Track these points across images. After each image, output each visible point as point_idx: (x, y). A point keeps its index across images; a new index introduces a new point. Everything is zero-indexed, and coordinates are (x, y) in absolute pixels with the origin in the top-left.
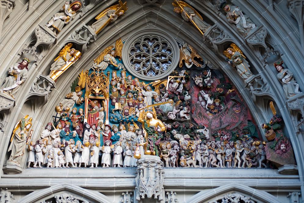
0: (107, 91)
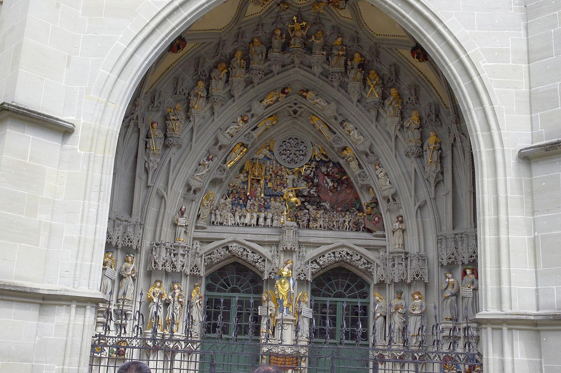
0: (263, 173)
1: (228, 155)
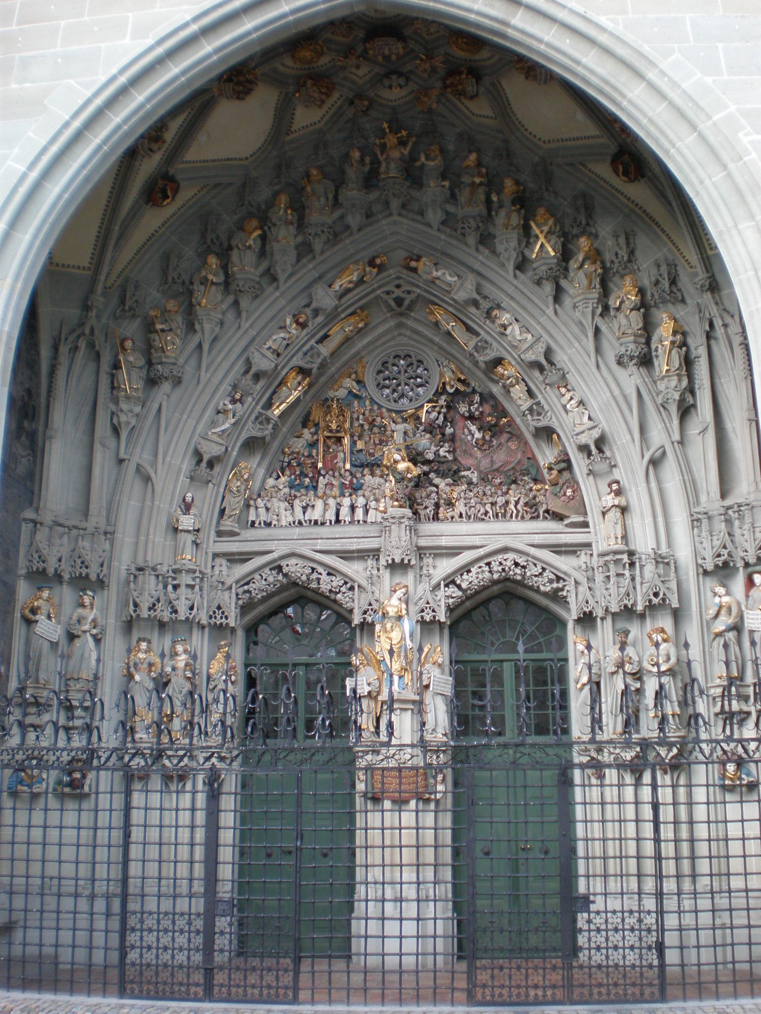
0: (347, 425)
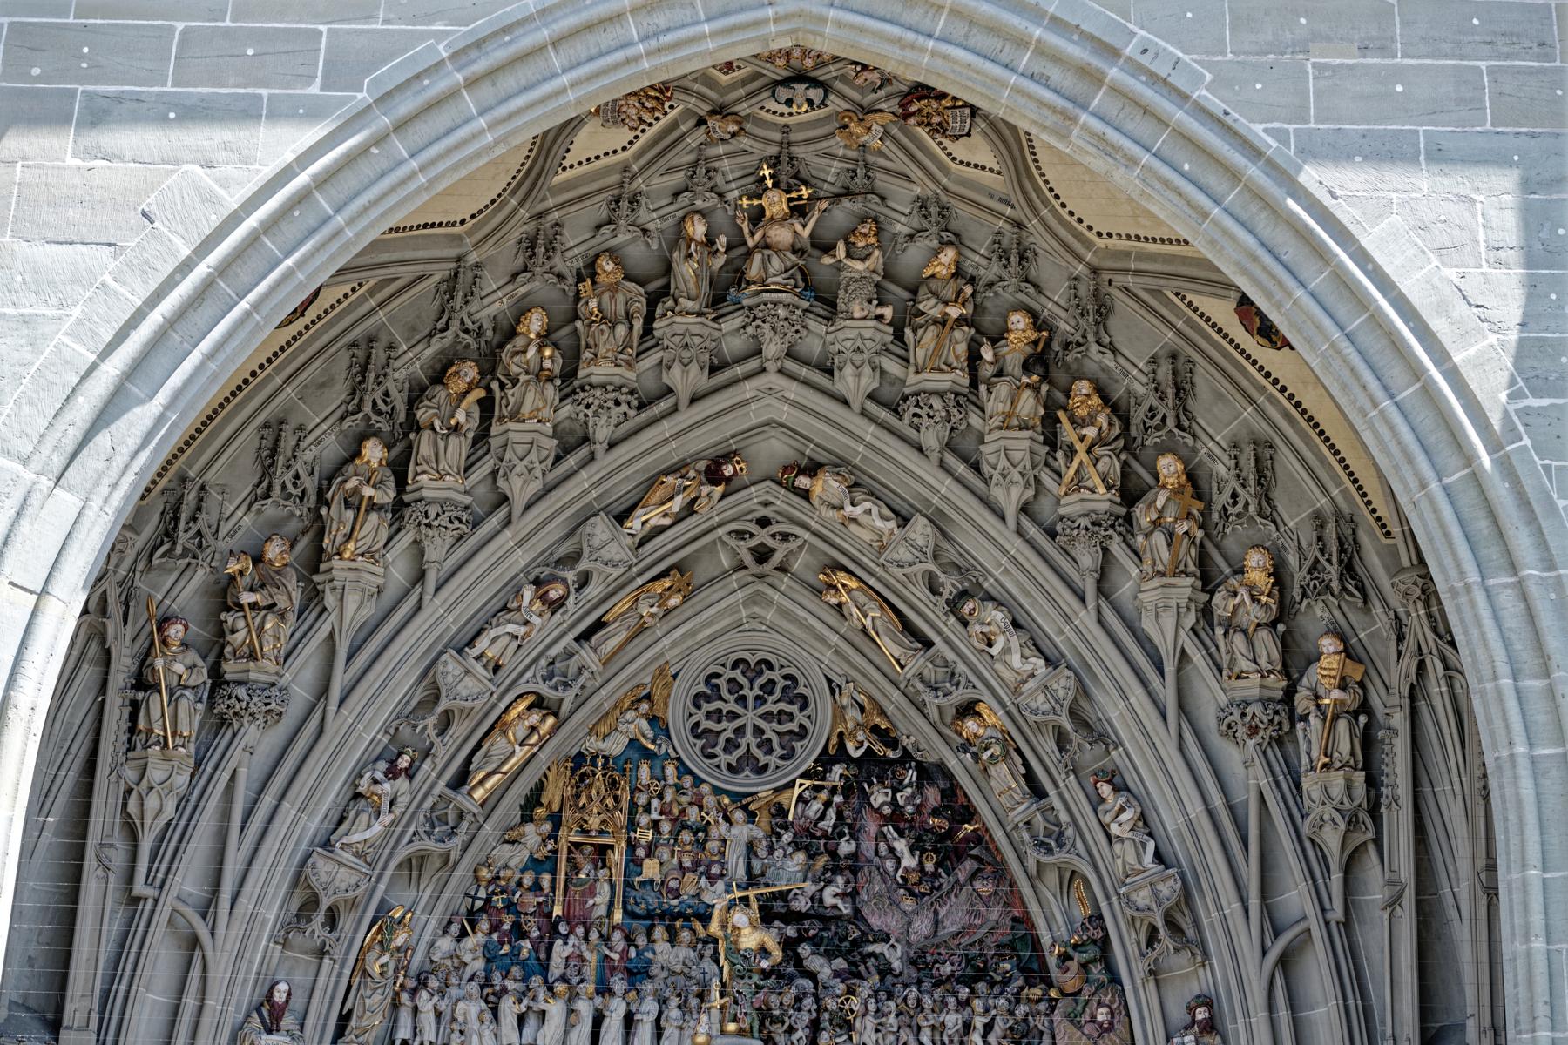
1: (478, 746)
